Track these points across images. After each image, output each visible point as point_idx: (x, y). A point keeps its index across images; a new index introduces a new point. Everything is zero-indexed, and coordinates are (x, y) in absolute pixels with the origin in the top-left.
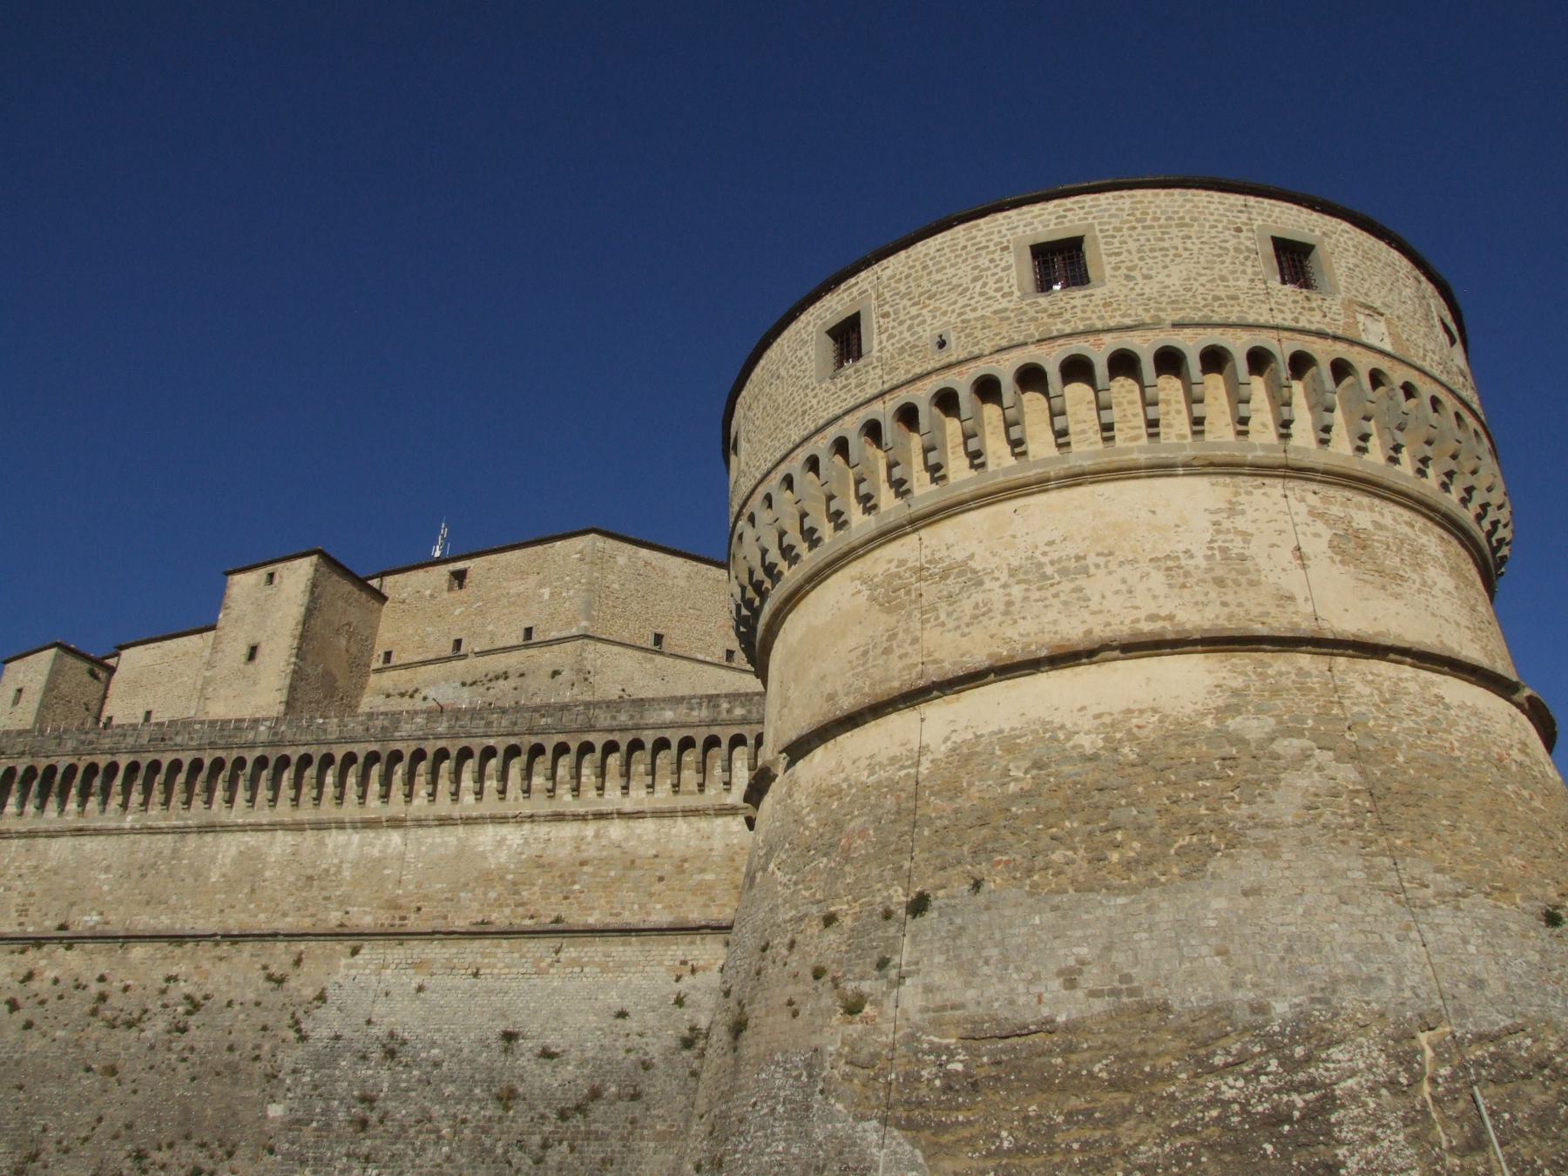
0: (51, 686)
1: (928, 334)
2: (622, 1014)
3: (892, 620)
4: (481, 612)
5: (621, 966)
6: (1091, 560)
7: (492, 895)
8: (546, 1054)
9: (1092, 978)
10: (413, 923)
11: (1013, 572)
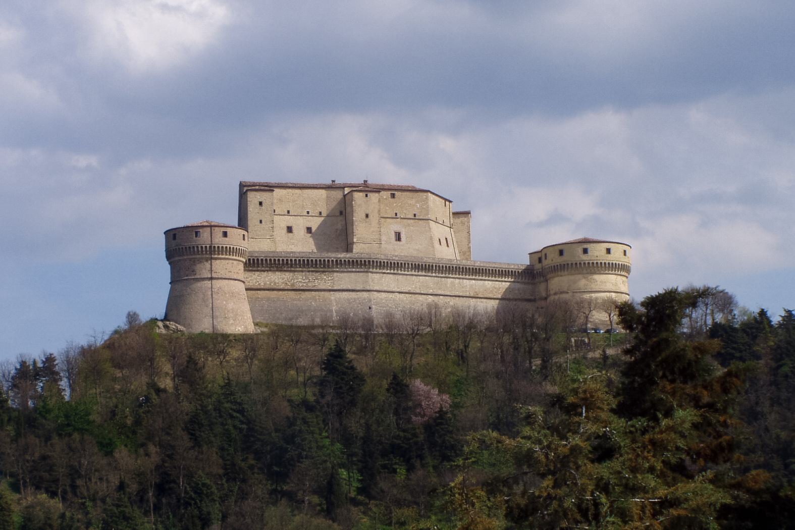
1: (595, 255)
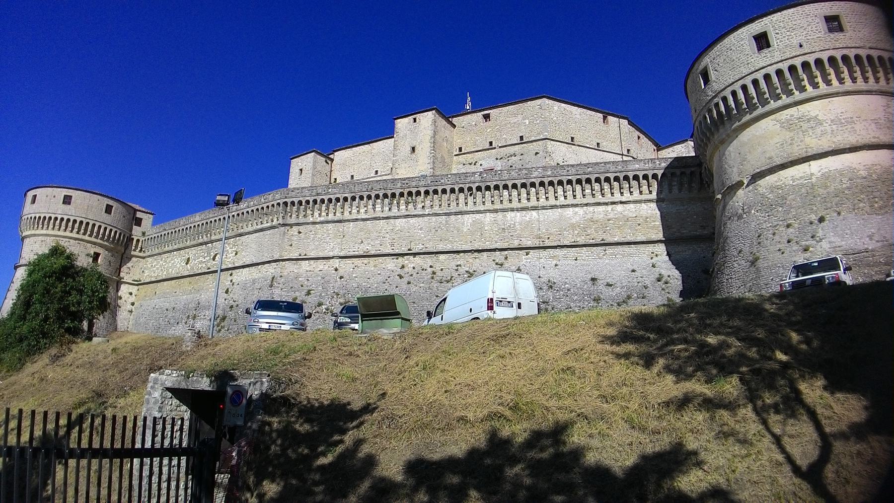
0: (314, 168)
1: (795, 42)
2: (633, 271)
3: (792, 134)
4: (498, 130)
5: (630, 255)
6: (855, 119)
8: (609, 285)
9: (876, 238)
10: (547, 243)
11: (832, 121)
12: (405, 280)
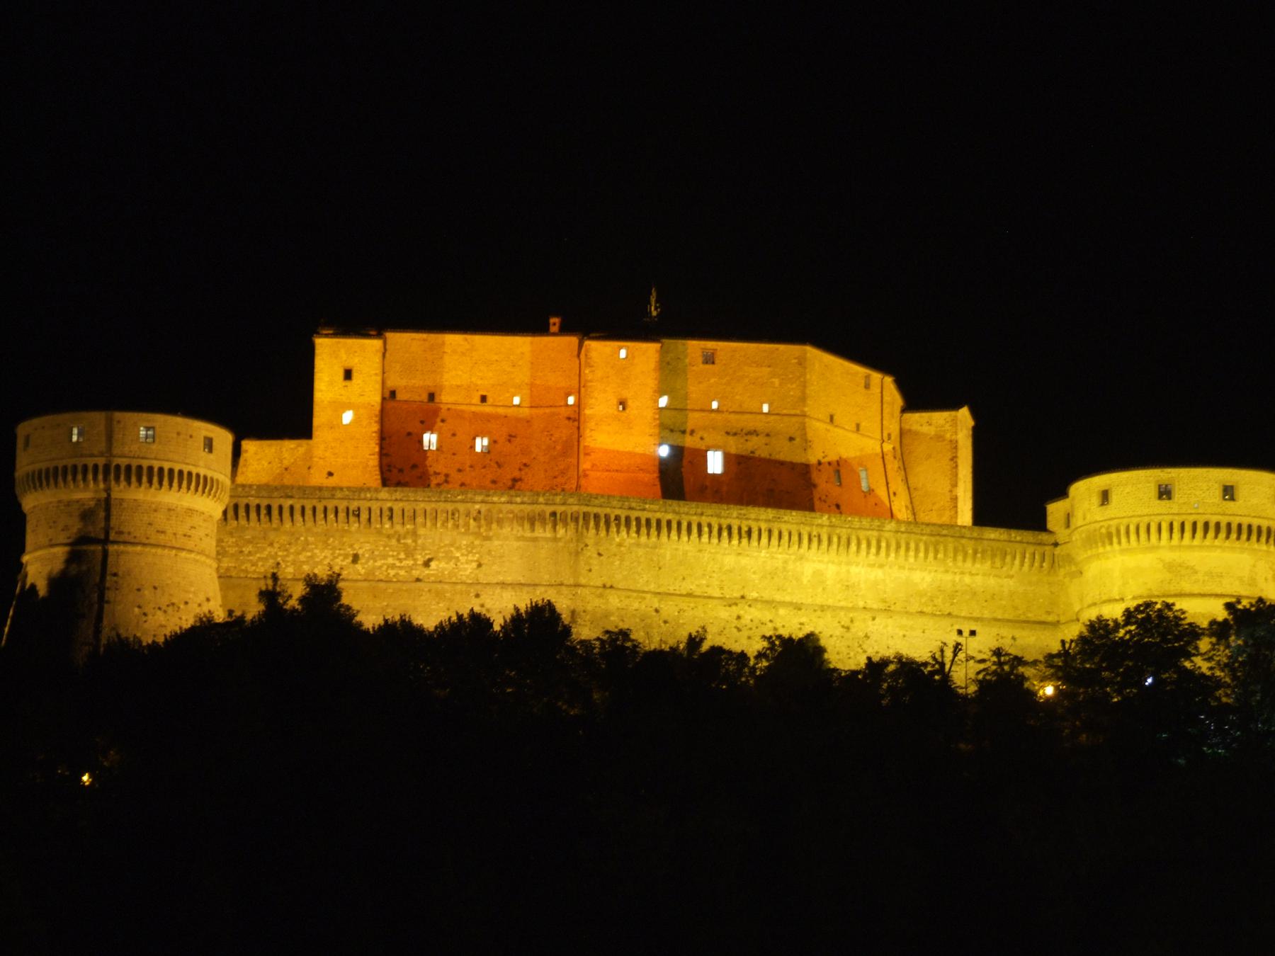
7: (923, 600)
12: (745, 633)
